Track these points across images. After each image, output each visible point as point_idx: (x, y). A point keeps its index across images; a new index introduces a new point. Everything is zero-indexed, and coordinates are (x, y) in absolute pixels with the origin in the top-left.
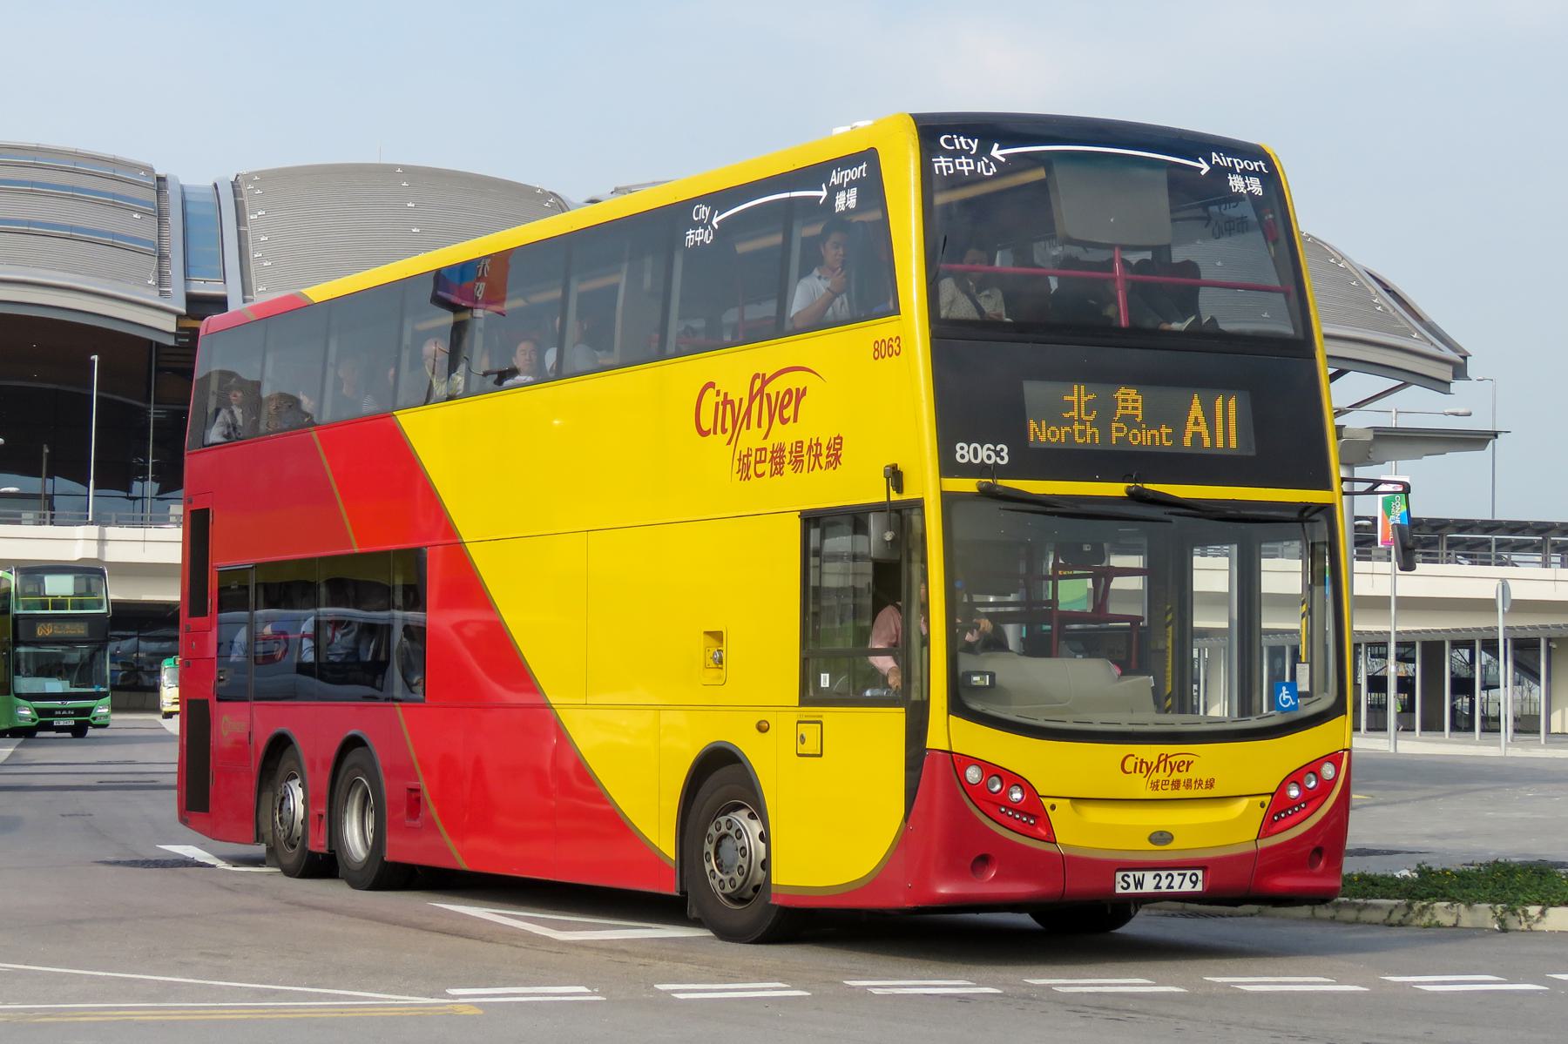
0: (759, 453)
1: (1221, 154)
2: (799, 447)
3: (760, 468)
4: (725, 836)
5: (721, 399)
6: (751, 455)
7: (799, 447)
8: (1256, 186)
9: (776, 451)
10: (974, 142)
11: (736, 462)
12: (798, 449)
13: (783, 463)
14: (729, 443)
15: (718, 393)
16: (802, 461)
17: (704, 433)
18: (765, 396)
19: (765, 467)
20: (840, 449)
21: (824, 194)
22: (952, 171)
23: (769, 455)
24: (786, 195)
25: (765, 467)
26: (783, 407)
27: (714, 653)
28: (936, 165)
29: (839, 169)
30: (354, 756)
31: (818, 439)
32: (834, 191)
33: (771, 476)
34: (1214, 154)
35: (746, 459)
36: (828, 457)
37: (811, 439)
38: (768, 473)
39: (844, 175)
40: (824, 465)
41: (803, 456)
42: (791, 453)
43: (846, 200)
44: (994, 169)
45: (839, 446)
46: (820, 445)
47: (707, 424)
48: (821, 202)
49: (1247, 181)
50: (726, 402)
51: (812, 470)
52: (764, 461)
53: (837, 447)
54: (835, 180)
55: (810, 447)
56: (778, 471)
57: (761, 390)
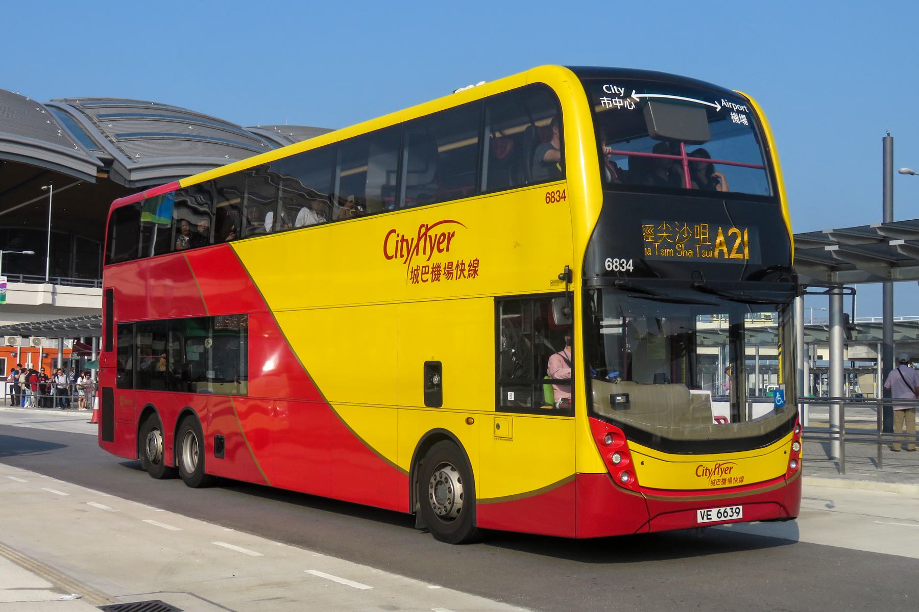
0: (424, 269)
2: (450, 265)
3: (425, 277)
5: (400, 238)
6: (419, 270)
7: (450, 265)
9: (435, 268)
11: (410, 274)
12: (449, 267)
13: (440, 274)
14: (405, 263)
15: (398, 235)
16: (453, 273)
17: (391, 258)
18: (428, 238)
19: (429, 276)
20: (478, 267)
23: (431, 270)
25: (429, 276)
26: (439, 243)
30: (188, 420)
31: (462, 261)
33: (432, 281)
35: (416, 272)
36: (469, 271)
37: (458, 261)
38: (430, 280)
40: (467, 276)
41: (453, 270)
42: (445, 268)
45: (477, 265)
46: (464, 264)
47: (391, 252)
50: (403, 240)
51: (459, 278)
52: (428, 273)
53: (477, 265)
55: (458, 266)
56: (436, 277)
57: (425, 234)
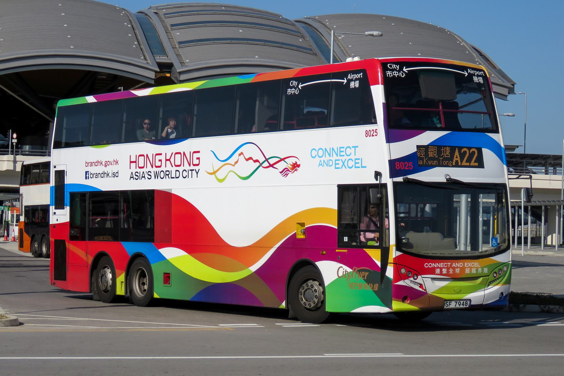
1: (471, 69)
4: (309, 289)
8: (481, 81)
10: (398, 66)
21: (345, 81)
22: (392, 76)
24: (330, 80)
27: (301, 230)
28: (387, 74)
29: (351, 74)
32: (349, 81)
34: (469, 69)
39: (353, 76)
43: (354, 85)
44: (404, 75)
48: (344, 84)
49: (479, 78)
54: (350, 77)
